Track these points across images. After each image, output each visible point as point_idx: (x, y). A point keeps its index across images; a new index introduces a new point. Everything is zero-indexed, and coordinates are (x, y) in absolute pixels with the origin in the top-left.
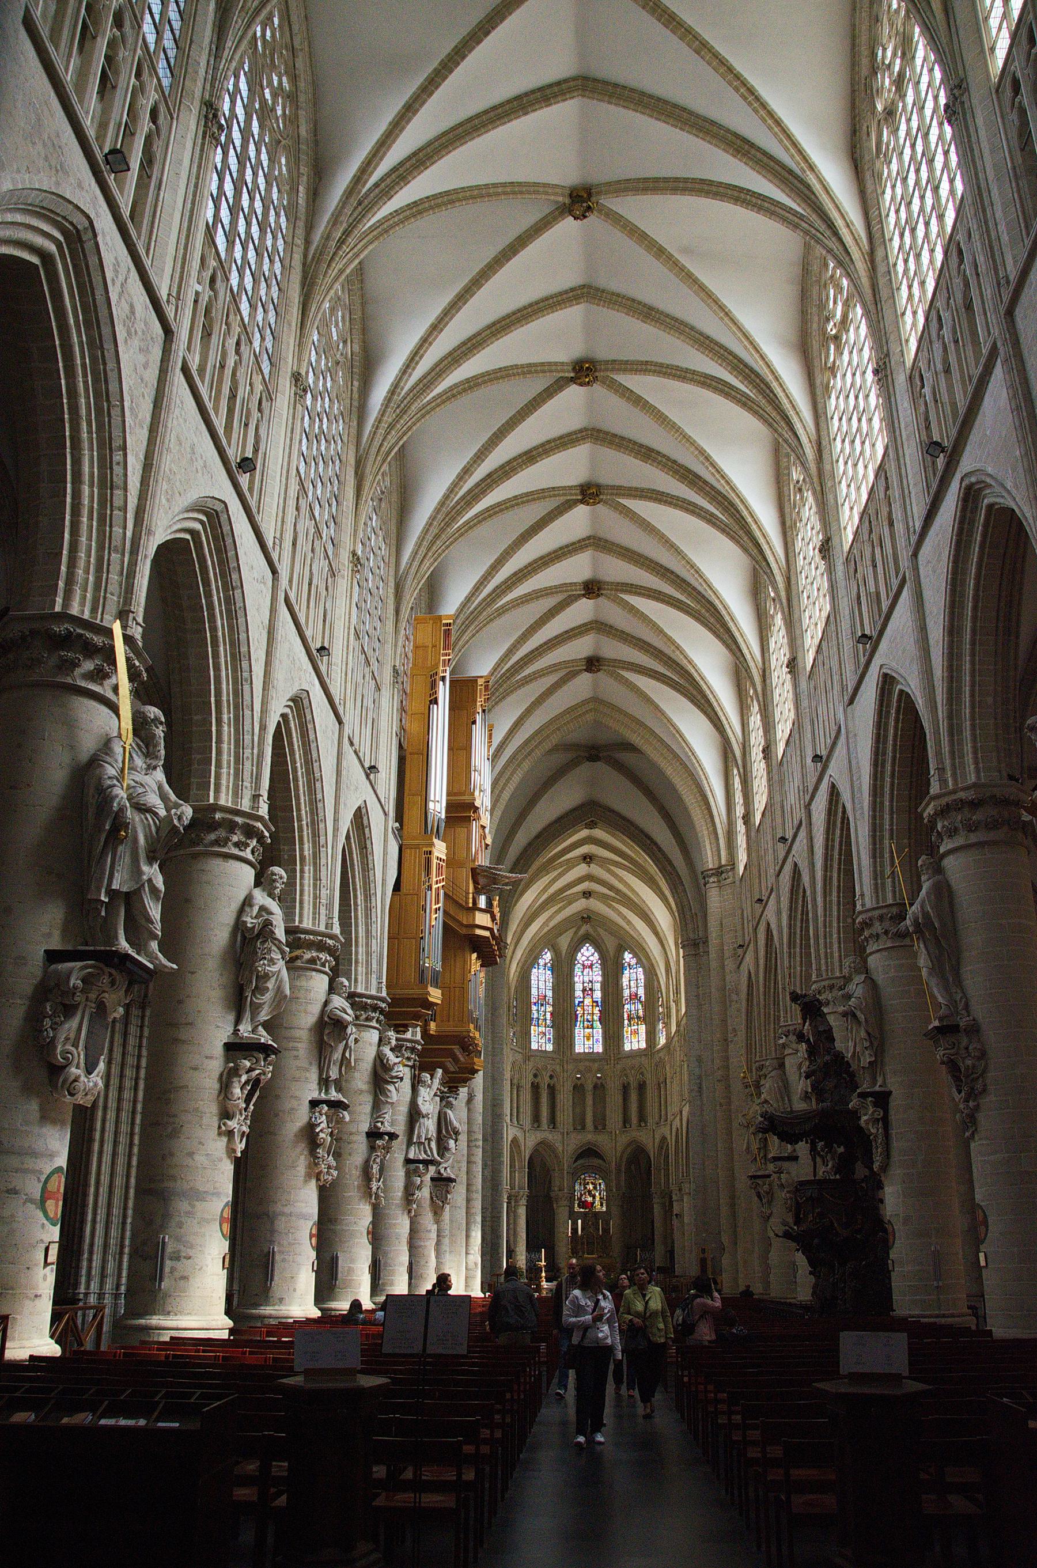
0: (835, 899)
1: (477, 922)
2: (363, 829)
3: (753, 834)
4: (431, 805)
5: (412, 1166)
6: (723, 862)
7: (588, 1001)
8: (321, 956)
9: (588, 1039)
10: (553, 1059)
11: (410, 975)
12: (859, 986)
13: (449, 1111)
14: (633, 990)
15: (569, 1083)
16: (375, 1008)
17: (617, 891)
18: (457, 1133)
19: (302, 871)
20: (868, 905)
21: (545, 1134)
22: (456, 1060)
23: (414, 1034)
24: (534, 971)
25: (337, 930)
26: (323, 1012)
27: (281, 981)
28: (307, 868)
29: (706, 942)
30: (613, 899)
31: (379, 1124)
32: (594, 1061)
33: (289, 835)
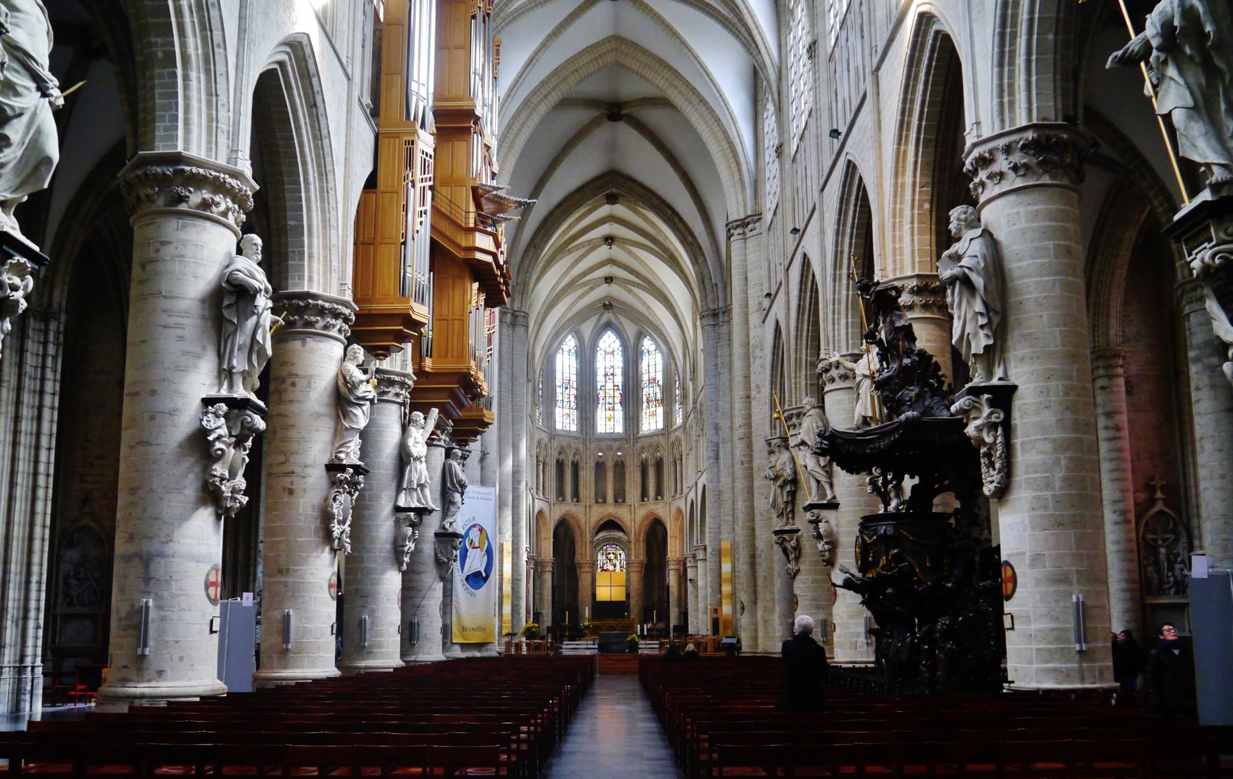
0: (908, 179)
1: (478, 244)
2: (310, 78)
3: (788, 165)
4: (414, 86)
5: (403, 515)
6: (749, 213)
7: (609, 385)
8: (217, 198)
9: (610, 420)
10: (577, 438)
11: (387, 285)
12: (973, 242)
13: (456, 466)
14: (652, 375)
15: (592, 460)
16: (336, 315)
17: (638, 275)
18: (463, 486)
19: (186, 78)
20: (986, 134)
21: (568, 507)
22: (461, 406)
23: (404, 366)
24: (559, 357)
25: (245, 166)
26: (222, 275)
27: (39, 132)
28: (193, 75)
29: (727, 311)
30: (634, 284)
31: (342, 456)
32: (615, 440)
33: (161, 20)
